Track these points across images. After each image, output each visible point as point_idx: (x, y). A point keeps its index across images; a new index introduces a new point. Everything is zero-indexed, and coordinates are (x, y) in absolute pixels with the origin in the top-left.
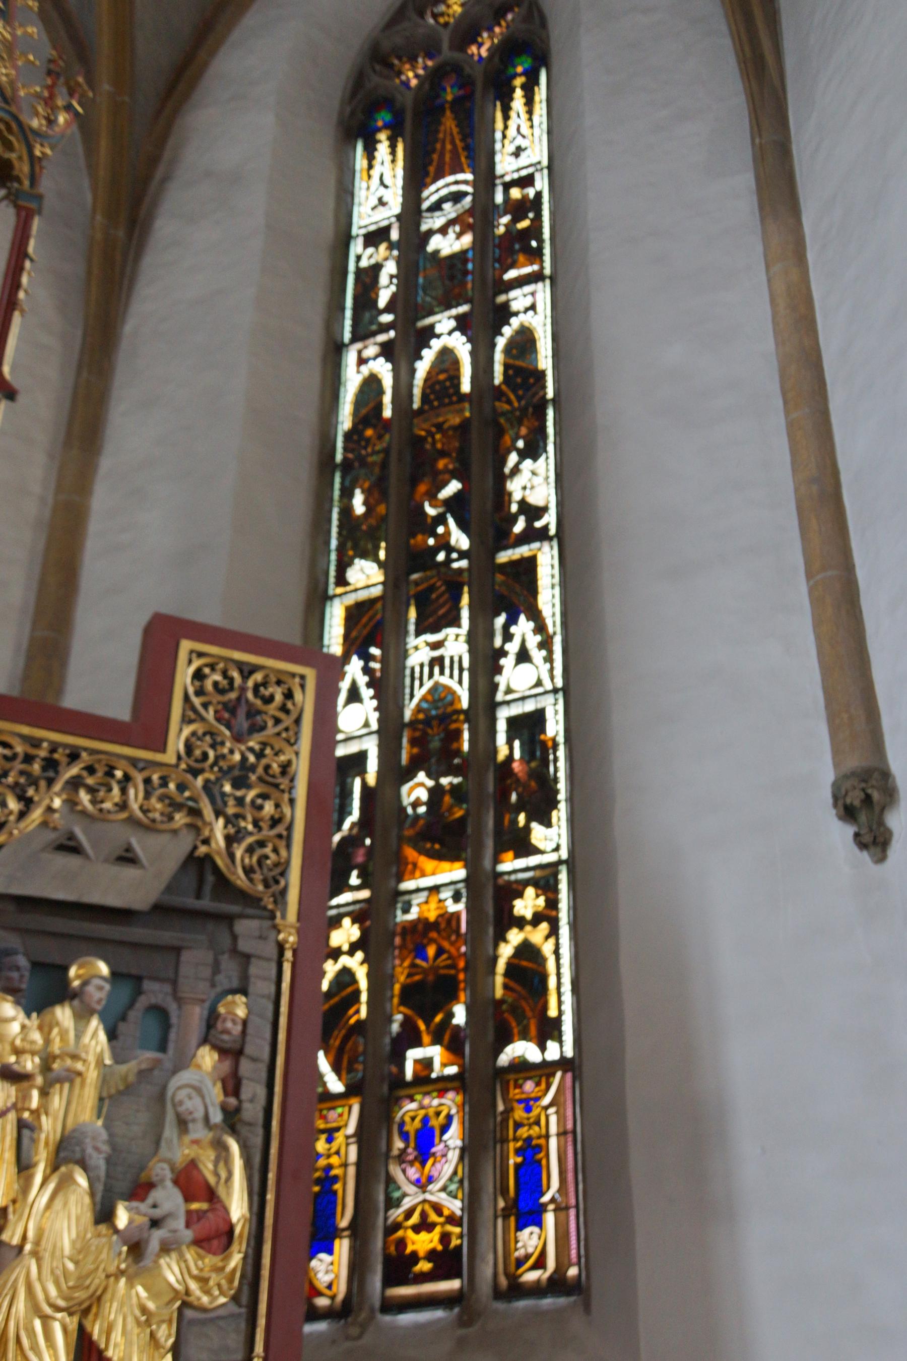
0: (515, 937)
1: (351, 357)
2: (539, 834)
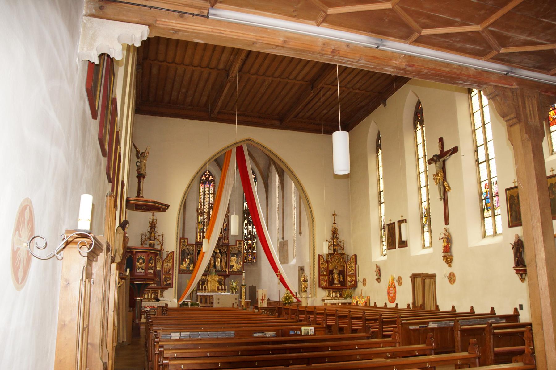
0: (254, 245)
1: (245, 203)
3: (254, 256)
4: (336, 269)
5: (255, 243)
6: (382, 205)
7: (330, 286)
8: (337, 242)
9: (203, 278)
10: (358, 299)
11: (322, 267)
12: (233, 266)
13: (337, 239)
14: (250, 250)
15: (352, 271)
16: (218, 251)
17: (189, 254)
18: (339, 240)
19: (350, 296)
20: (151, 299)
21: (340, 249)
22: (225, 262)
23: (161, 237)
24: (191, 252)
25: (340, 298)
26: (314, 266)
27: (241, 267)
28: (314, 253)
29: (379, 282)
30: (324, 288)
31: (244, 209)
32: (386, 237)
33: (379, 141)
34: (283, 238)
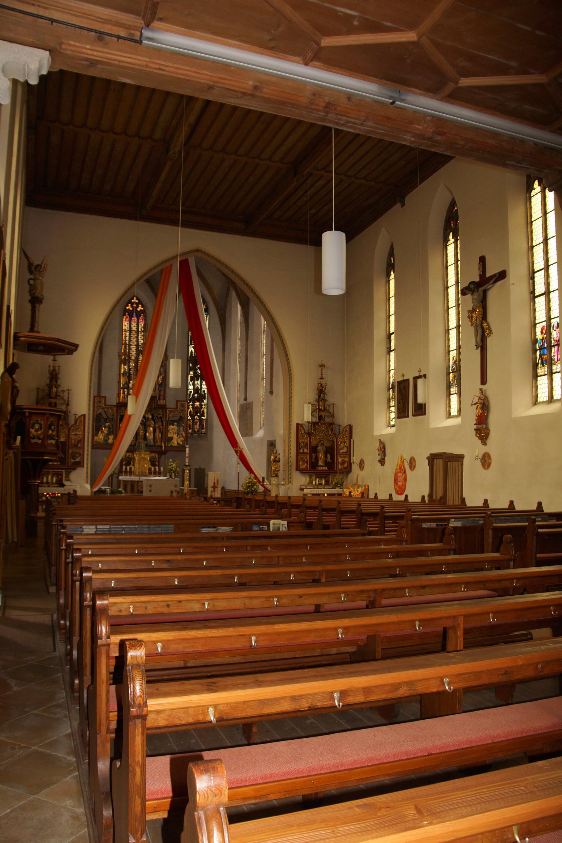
0: (203, 409)
1: (190, 347)
2: (204, 401)
3: (203, 425)
4: (321, 444)
5: (205, 405)
6: (392, 354)
7: (312, 469)
8: (324, 406)
9: (128, 455)
10: (352, 489)
11: (302, 442)
12: (172, 438)
13: (325, 402)
14: (198, 416)
15: (345, 448)
16: (150, 417)
17: (108, 421)
18: (327, 403)
19: (340, 485)
20: (53, 484)
21: (328, 417)
22: (160, 432)
23: (66, 393)
24: (110, 417)
25: (326, 487)
26: (290, 439)
27: (183, 440)
28: (290, 421)
29: (383, 465)
30: (303, 472)
31: (190, 355)
32: (395, 400)
33: (392, 258)
34: (246, 399)
